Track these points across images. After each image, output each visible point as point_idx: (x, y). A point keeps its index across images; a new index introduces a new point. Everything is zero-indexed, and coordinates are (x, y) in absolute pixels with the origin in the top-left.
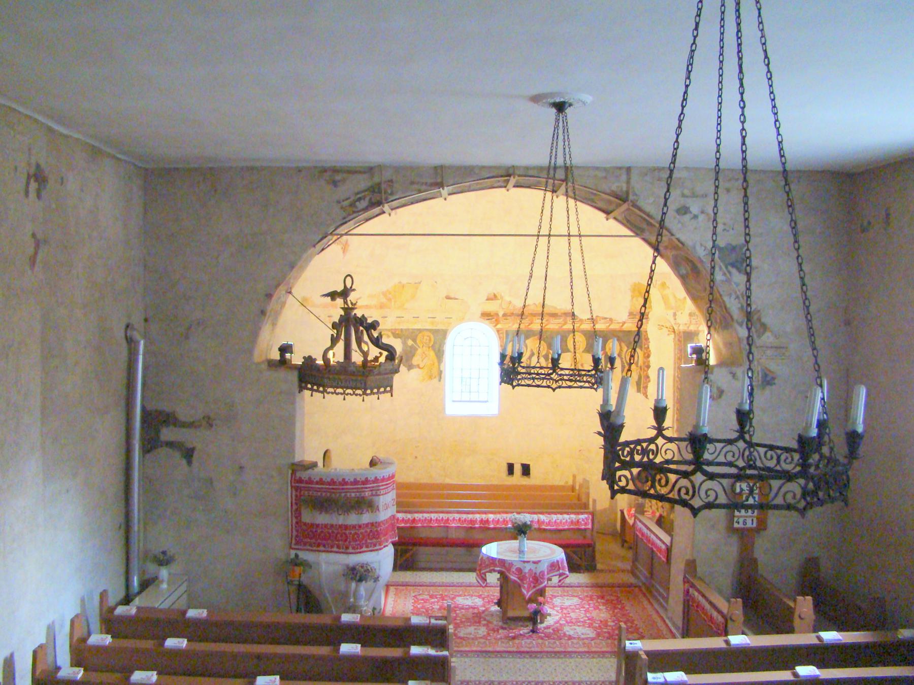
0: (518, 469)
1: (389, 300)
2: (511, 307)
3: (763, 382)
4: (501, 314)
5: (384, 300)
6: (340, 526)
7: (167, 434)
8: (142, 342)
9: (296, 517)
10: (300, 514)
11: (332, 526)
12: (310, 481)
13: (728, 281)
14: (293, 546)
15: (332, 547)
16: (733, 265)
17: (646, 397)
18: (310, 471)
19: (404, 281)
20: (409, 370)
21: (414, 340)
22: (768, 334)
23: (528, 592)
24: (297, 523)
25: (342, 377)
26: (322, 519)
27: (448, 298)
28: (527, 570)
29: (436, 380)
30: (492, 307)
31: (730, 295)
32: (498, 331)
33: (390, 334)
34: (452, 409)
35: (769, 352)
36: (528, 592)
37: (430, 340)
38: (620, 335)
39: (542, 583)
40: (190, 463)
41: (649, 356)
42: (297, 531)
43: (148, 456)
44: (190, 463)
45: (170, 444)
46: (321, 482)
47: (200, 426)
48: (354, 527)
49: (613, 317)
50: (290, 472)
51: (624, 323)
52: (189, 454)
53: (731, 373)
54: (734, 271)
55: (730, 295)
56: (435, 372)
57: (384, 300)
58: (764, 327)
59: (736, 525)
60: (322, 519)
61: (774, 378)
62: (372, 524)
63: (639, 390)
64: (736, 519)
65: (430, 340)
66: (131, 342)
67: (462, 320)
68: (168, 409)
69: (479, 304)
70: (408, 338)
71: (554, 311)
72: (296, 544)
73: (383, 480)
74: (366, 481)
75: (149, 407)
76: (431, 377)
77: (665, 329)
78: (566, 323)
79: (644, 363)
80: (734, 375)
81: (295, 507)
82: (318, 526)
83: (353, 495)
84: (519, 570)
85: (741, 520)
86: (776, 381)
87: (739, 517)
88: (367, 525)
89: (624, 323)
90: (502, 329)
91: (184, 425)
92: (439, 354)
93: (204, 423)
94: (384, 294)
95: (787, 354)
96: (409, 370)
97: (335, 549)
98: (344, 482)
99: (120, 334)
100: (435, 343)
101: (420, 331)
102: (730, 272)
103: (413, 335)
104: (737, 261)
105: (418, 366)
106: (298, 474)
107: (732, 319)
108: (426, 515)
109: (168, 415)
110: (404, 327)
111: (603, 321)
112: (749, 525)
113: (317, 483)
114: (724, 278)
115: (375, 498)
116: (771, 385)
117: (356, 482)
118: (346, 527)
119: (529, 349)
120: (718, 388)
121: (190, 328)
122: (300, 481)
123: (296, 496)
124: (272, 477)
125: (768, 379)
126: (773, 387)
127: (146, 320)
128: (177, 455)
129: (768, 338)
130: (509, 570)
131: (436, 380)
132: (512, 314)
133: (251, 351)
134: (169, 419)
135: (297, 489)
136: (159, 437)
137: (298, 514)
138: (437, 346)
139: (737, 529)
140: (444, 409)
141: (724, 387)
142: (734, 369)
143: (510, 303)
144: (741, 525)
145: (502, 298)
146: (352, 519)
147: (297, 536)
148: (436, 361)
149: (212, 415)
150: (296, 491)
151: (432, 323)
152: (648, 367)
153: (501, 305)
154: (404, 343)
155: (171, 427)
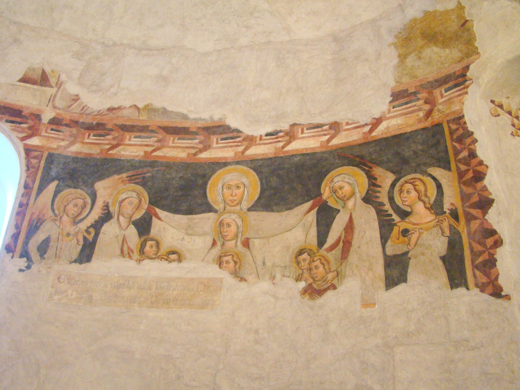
2: (76, 108)
4: (47, 116)
17: (497, 293)
30: (26, 98)
32: (28, 151)
41: (479, 177)
49: (340, 115)
51: (377, 122)
63: (456, 278)
71: (179, 123)
77: (506, 119)
78: (207, 147)
79: (464, 197)
89: (377, 122)
90: (36, 148)
111: (307, 133)
132: (75, 123)
143: (76, 98)
145: (59, 84)
152: (485, 203)
153: (52, 99)
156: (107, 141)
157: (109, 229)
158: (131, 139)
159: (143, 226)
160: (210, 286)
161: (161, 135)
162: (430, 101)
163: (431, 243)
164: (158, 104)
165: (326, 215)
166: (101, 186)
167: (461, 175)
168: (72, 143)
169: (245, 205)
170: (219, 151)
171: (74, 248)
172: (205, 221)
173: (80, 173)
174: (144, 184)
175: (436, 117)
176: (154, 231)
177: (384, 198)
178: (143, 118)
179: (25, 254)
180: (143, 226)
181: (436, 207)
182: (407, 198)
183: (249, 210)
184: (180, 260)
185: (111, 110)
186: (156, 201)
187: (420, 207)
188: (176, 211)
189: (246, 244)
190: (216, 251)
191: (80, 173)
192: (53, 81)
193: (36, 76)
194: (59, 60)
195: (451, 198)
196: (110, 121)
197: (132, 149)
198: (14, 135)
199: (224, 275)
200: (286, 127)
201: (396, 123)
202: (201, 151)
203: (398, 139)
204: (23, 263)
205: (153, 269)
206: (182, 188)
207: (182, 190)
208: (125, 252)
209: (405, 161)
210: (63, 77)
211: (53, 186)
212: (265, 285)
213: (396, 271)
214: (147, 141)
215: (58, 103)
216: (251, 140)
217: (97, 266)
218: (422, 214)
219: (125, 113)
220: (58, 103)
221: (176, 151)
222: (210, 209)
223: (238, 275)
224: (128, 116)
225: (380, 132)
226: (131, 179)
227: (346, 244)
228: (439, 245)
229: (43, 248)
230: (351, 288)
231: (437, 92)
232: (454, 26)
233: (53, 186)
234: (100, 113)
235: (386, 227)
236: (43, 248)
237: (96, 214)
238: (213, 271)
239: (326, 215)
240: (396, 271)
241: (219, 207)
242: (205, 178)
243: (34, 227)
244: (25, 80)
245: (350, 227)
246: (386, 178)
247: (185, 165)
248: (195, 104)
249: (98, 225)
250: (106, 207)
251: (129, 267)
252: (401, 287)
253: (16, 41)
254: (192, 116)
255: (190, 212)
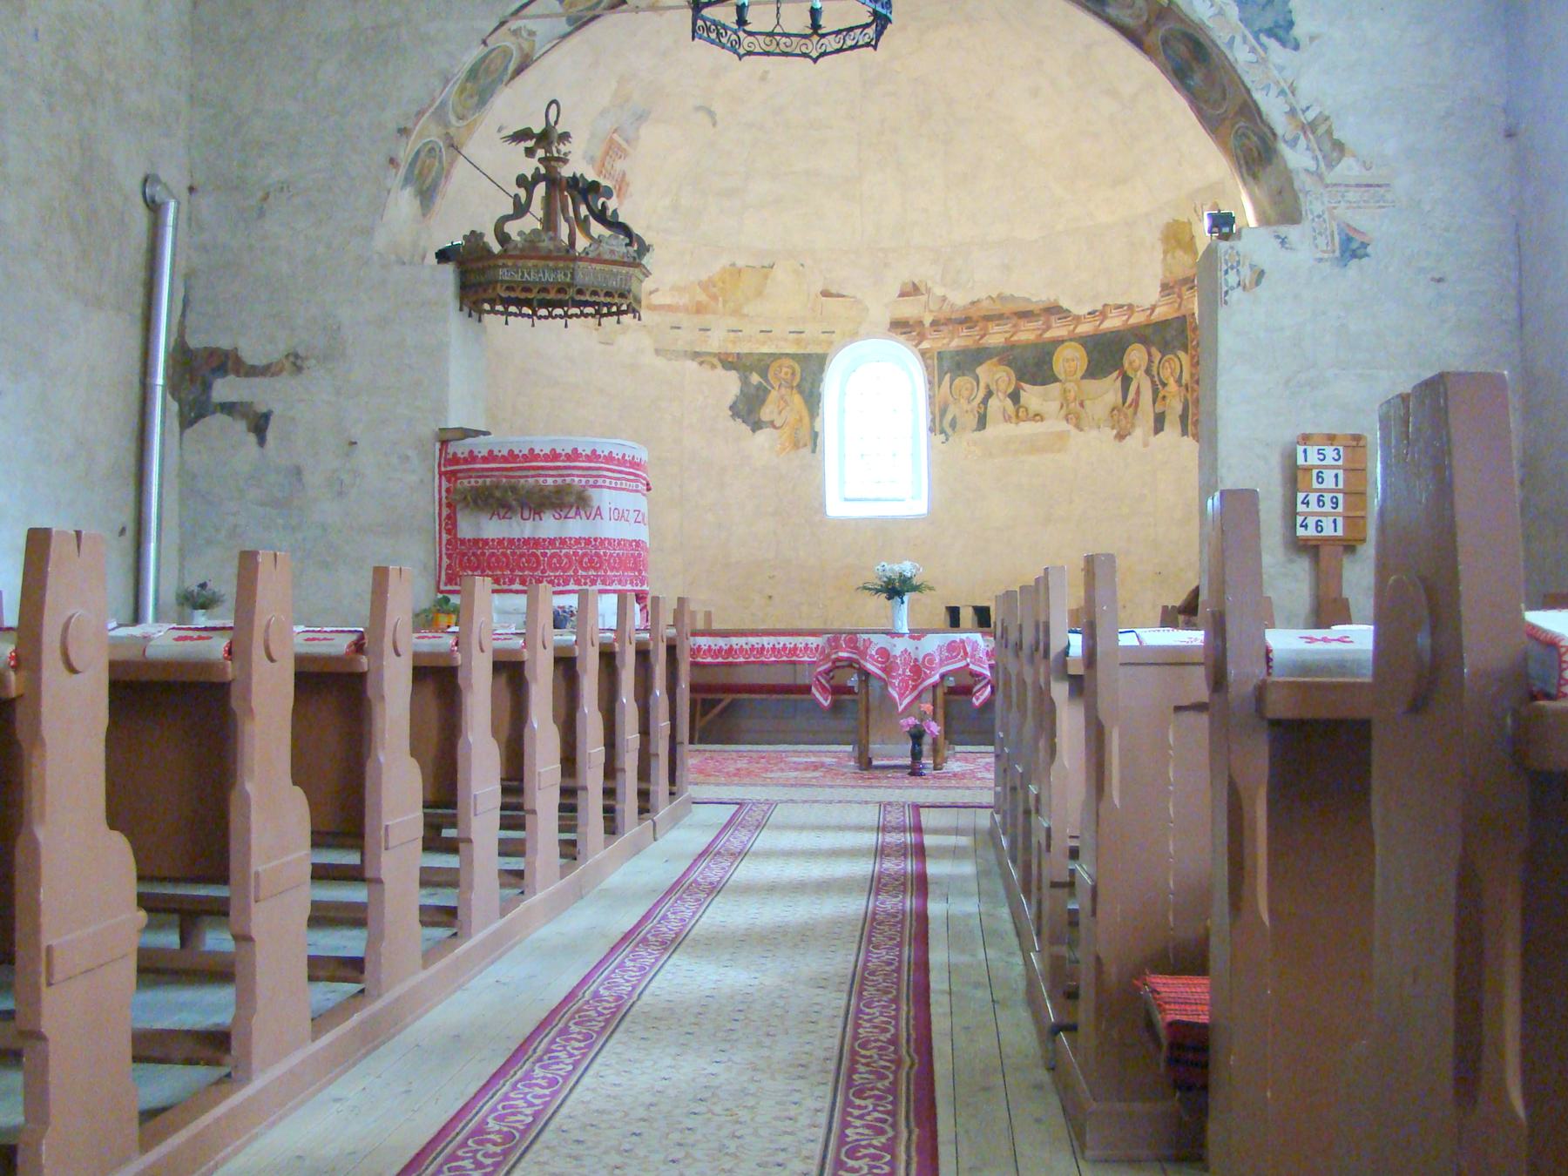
0: (967, 616)
1: (714, 298)
2: (946, 307)
3: (1343, 252)
4: (927, 320)
5: (703, 298)
6: (526, 541)
7: (225, 389)
8: (172, 205)
9: (449, 532)
10: (455, 525)
11: (511, 541)
12: (472, 458)
13: (1262, 62)
14: (442, 587)
15: (512, 582)
16: (1271, 33)
18: (469, 440)
19: (740, 263)
20: (754, 431)
21: (764, 373)
22: (1347, 161)
23: (902, 696)
24: (449, 542)
25: (530, 263)
26: (493, 528)
27: (826, 294)
28: (898, 653)
29: (806, 451)
30: (909, 309)
31: (1267, 88)
32: (923, 353)
33: (715, 361)
34: (836, 508)
35: (1352, 195)
36: (902, 696)
37: (793, 374)
38: (1149, 331)
39: (928, 677)
40: (262, 441)
42: (449, 556)
43: (189, 432)
44: (262, 441)
45: (229, 408)
46: (491, 457)
47: (281, 371)
48: (552, 541)
50: (438, 446)
51: (1153, 308)
52: (260, 425)
53: (1278, 237)
54: (1272, 44)
55: (1267, 88)
56: (804, 433)
57: (703, 298)
58: (1339, 147)
59: (1300, 532)
60: (493, 528)
61: (1364, 245)
62: (588, 541)
63: (1184, 432)
64: (1299, 519)
65: (793, 374)
66: (155, 208)
67: (854, 336)
68: (225, 343)
69: (882, 305)
70: (752, 369)
72: (450, 580)
73: (609, 458)
74: (575, 455)
75: (194, 342)
76: (796, 445)
78: (1049, 328)
79: (1192, 375)
80: (1283, 242)
81: (445, 512)
82: (486, 542)
83: (550, 481)
84: (884, 653)
85: (1311, 521)
86: (1369, 250)
87: (1306, 515)
88: (578, 541)
89: (1153, 308)
91: (254, 371)
92: (812, 400)
93: (287, 365)
94: (705, 286)
95: (1389, 197)
96: (754, 431)
97: (517, 586)
98: (532, 455)
99: (134, 184)
100: (802, 379)
101: (775, 357)
102: (1261, 44)
103: (762, 364)
104: (1277, 26)
105: (772, 424)
106: (451, 450)
107: (1275, 135)
108: (753, 640)
109: (226, 354)
110: (744, 348)
112: (1328, 531)
113: (485, 460)
114: (1252, 57)
115: (594, 494)
116: (1361, 257)
117: (555, 456)
118: (537, 542)
119: (982, 384)
120: (1252, 267)
121: (266, 198)
122: (455, 460)
123: (448, 491)
124: (408, 458)
125: (1354, 245)
126: (1365, 260)
127: (191, 189)
128: (241, 426)
129: (1348, 169)
130: (863, 654)
131: (806, 451)
132: (948, 321)
133: (368, 232)
134: (226, 362)
135: (451, 476)
136: (209, 397)
137: (450, 524)
138: (807, 386)
139: (1307, 540)
140: (823, 505)
141: (1263, 261)
142: (1284, 230)
143: (944, 299)
144: (1311, 532)
145: (929, 291)
146: (548, 526)
147: (449, 567)
148: (805, 413)
149: (301, 352)
150: (449, 481)
151: (798, 342)
153: (926, 305)
154: (745, 381)
155: (231, 378)
156: (976, 332)
157: (994, 403)
158: (993, 328)
159: (1015, 397)
160: (1061, 436)
161: (1015, 320)
162: (1180, 296)
163: (1175, 406)
164: (1007, 292)
165: (1126, 381)
166: (980, 370)
167: (1193, 357)
168: (952, 339)
169: (1079, 374)
170: (1058, 331)
171: (973, 421)
172: (1054, 388)
173: (965, 362)
174: (1009, 365)
175: (1183, 311)
176: (1022, 401)
177: (1155, 372)
178: (998, 307)
179: (942, 431)
180: (1015, 397)
181: (1179, 381)
182: (1166, 374)
183: (1083, 377)
184: (1042, 420)
185: (973, 303)
186: (1020, 378)
187: (1171, 381)
188: (1034, 384)
189: (1082, 405)
190: (1063, 412)
191: (965, 362)
192: (923, 289)
193: (909, 288)
194: (925, 272)
195: (1186, 377)
196: (973, 313)
197: (996, 337)
198: (910, 344)
199: (1071, 427)
200: (1099, 307)
201: (1163, 312)
202: (1045, 331)
203: (1163, 325)
204: (943, 437)
205: (1028, 428)
206: (1037, 365)
207: (1034, 366)
208: (1007, 419)
209: (1166, 344)
210: (930, 284)
211: (947, 377)
212: (1094, 433)
213: (1159, 423)
214: (1007, 328)
215: (932, 307)
216: (1078, 319)
217: (990, 430)
218: (1172, 386)
219: (985, 304)
220: (932, 307)
221: (1027, 334)
222: (1056, 380)
223: (1078, 427)
224: (987, 307)
225: (1155, 317)
226: (1001, 362)
227: (1136, 403)
228: (1179, 408)
229: (953, 424)
230: (1138, 433)
231: (1184, 288)
232: (1187, 238)
233: (947, 377)
234: (965, 308)
235: (1155, 392)
236: (953, 424)
237: (981, 394)
238: (1063, 426)
239: (1126, 381)
240: (1159, 423)
241: (1062, 377)
242: (1051, 354)
243: (943, 412)
244: (902, 295)
245: (1138, 392)
246: (1157, 356)
247: (1035, 345)
248: (1033, 288)
249: (985, 401)
250: (988, 386)
251: (1011, 429)
252: (1161, 434)
253: (886, 265)
254: (1034, 299)
255: (1043, 384)
